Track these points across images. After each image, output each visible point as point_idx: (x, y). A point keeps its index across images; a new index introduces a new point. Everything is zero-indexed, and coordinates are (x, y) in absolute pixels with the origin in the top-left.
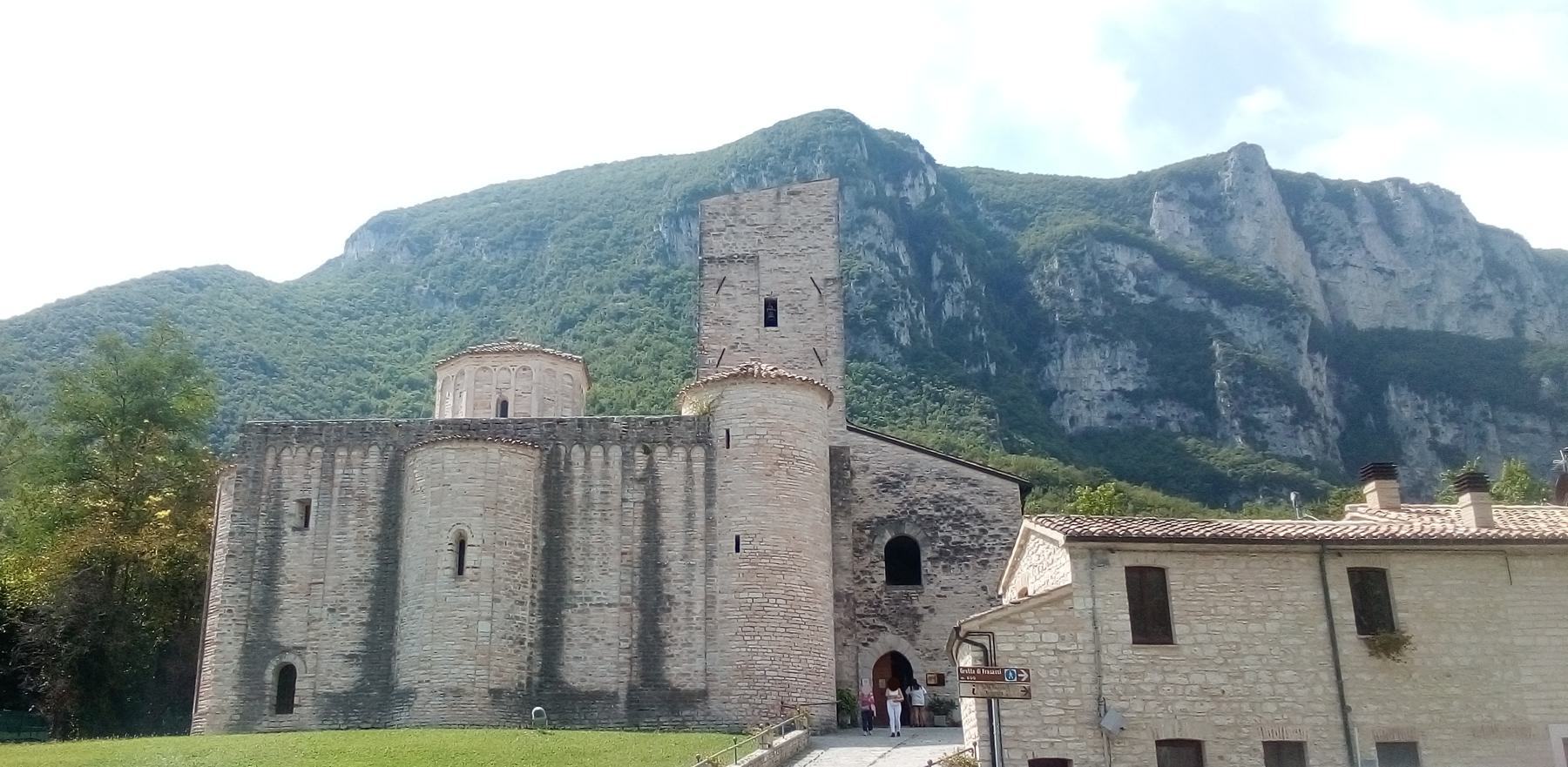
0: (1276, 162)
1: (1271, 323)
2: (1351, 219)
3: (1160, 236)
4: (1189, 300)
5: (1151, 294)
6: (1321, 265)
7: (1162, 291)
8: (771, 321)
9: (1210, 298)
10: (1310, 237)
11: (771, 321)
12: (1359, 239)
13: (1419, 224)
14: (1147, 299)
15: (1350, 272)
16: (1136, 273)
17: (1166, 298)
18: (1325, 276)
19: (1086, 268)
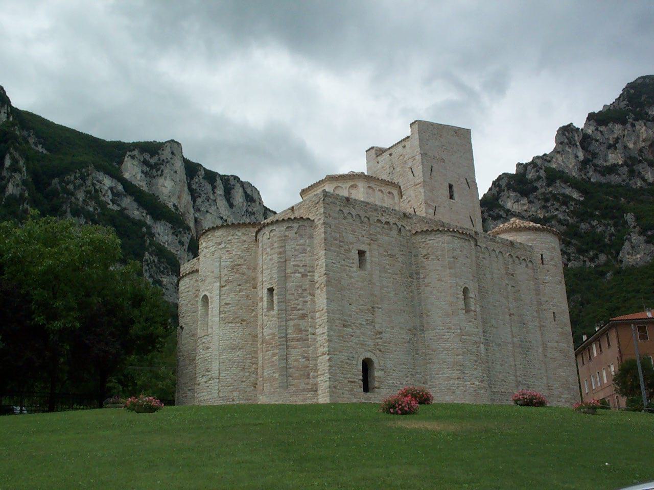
0: (186, 155)
1: (173, 233)
2: (213, 190)
3: (127, 175)
4: (136, 213)
5: (118, 205)
6: (198, 210)
7: (124, 206)
8: (451, 197)
9: (147, 214)
10: (194, 195)
11: (451, 197)
12: (215, 200)
13: (241, 200)
14: (115, 208)
15: (208, 216)
16: (112, 192)
17: (125, 209)
18: (197, 215)
19: (89, 183)
